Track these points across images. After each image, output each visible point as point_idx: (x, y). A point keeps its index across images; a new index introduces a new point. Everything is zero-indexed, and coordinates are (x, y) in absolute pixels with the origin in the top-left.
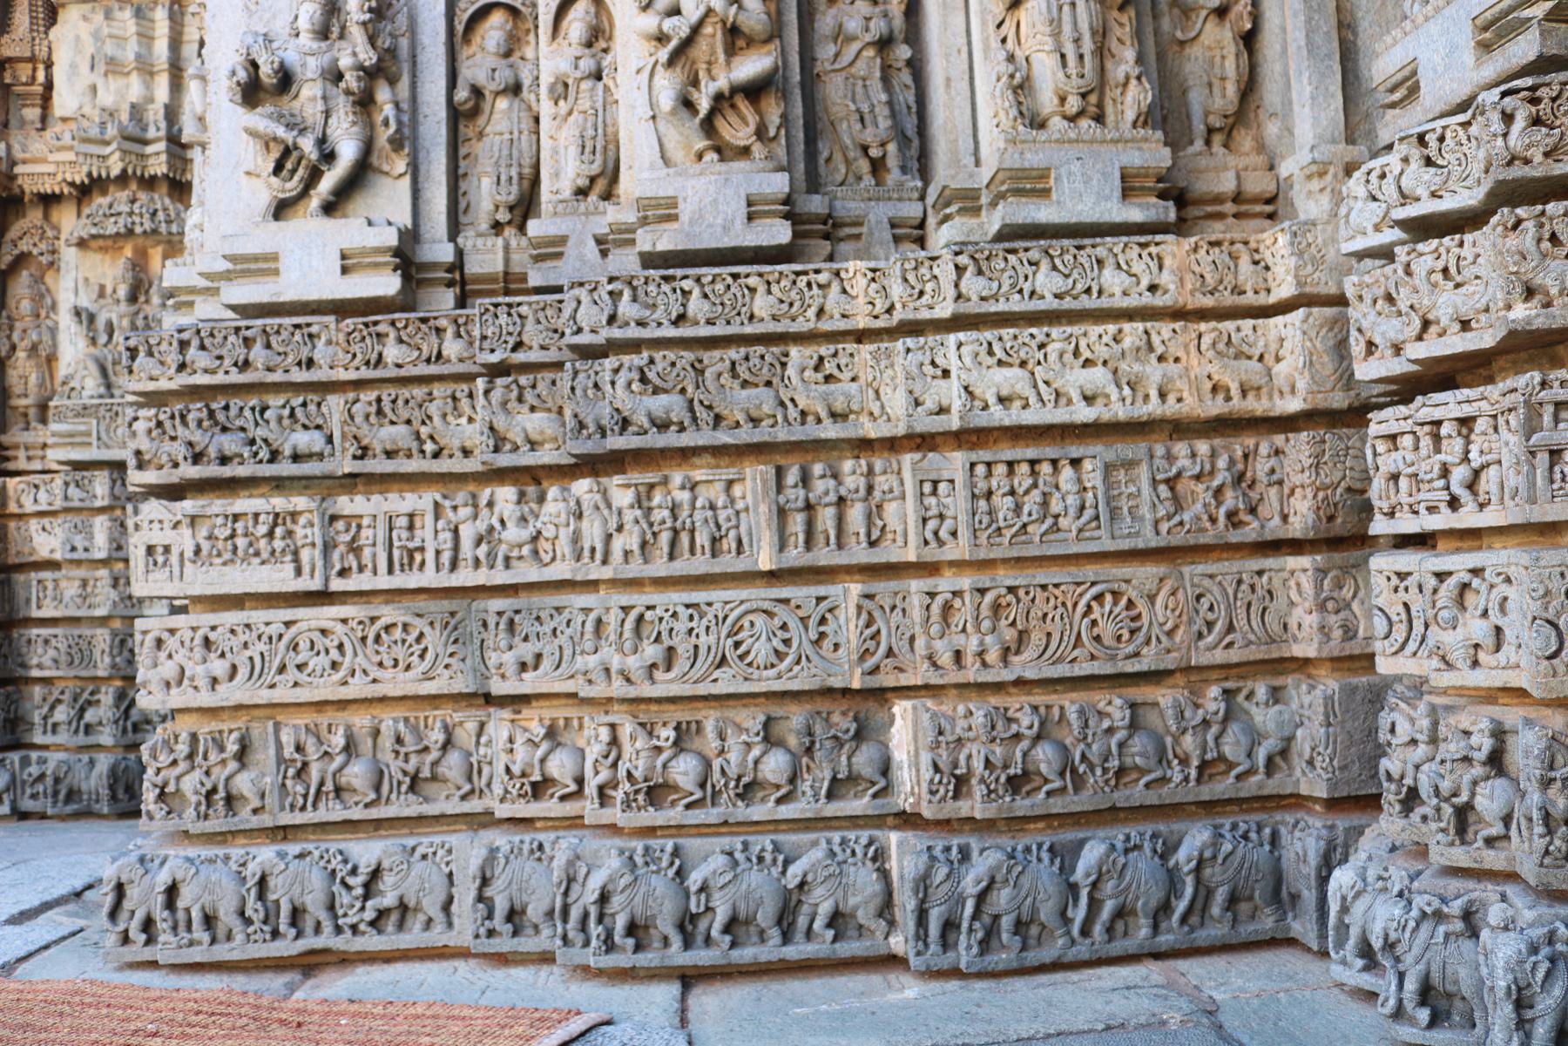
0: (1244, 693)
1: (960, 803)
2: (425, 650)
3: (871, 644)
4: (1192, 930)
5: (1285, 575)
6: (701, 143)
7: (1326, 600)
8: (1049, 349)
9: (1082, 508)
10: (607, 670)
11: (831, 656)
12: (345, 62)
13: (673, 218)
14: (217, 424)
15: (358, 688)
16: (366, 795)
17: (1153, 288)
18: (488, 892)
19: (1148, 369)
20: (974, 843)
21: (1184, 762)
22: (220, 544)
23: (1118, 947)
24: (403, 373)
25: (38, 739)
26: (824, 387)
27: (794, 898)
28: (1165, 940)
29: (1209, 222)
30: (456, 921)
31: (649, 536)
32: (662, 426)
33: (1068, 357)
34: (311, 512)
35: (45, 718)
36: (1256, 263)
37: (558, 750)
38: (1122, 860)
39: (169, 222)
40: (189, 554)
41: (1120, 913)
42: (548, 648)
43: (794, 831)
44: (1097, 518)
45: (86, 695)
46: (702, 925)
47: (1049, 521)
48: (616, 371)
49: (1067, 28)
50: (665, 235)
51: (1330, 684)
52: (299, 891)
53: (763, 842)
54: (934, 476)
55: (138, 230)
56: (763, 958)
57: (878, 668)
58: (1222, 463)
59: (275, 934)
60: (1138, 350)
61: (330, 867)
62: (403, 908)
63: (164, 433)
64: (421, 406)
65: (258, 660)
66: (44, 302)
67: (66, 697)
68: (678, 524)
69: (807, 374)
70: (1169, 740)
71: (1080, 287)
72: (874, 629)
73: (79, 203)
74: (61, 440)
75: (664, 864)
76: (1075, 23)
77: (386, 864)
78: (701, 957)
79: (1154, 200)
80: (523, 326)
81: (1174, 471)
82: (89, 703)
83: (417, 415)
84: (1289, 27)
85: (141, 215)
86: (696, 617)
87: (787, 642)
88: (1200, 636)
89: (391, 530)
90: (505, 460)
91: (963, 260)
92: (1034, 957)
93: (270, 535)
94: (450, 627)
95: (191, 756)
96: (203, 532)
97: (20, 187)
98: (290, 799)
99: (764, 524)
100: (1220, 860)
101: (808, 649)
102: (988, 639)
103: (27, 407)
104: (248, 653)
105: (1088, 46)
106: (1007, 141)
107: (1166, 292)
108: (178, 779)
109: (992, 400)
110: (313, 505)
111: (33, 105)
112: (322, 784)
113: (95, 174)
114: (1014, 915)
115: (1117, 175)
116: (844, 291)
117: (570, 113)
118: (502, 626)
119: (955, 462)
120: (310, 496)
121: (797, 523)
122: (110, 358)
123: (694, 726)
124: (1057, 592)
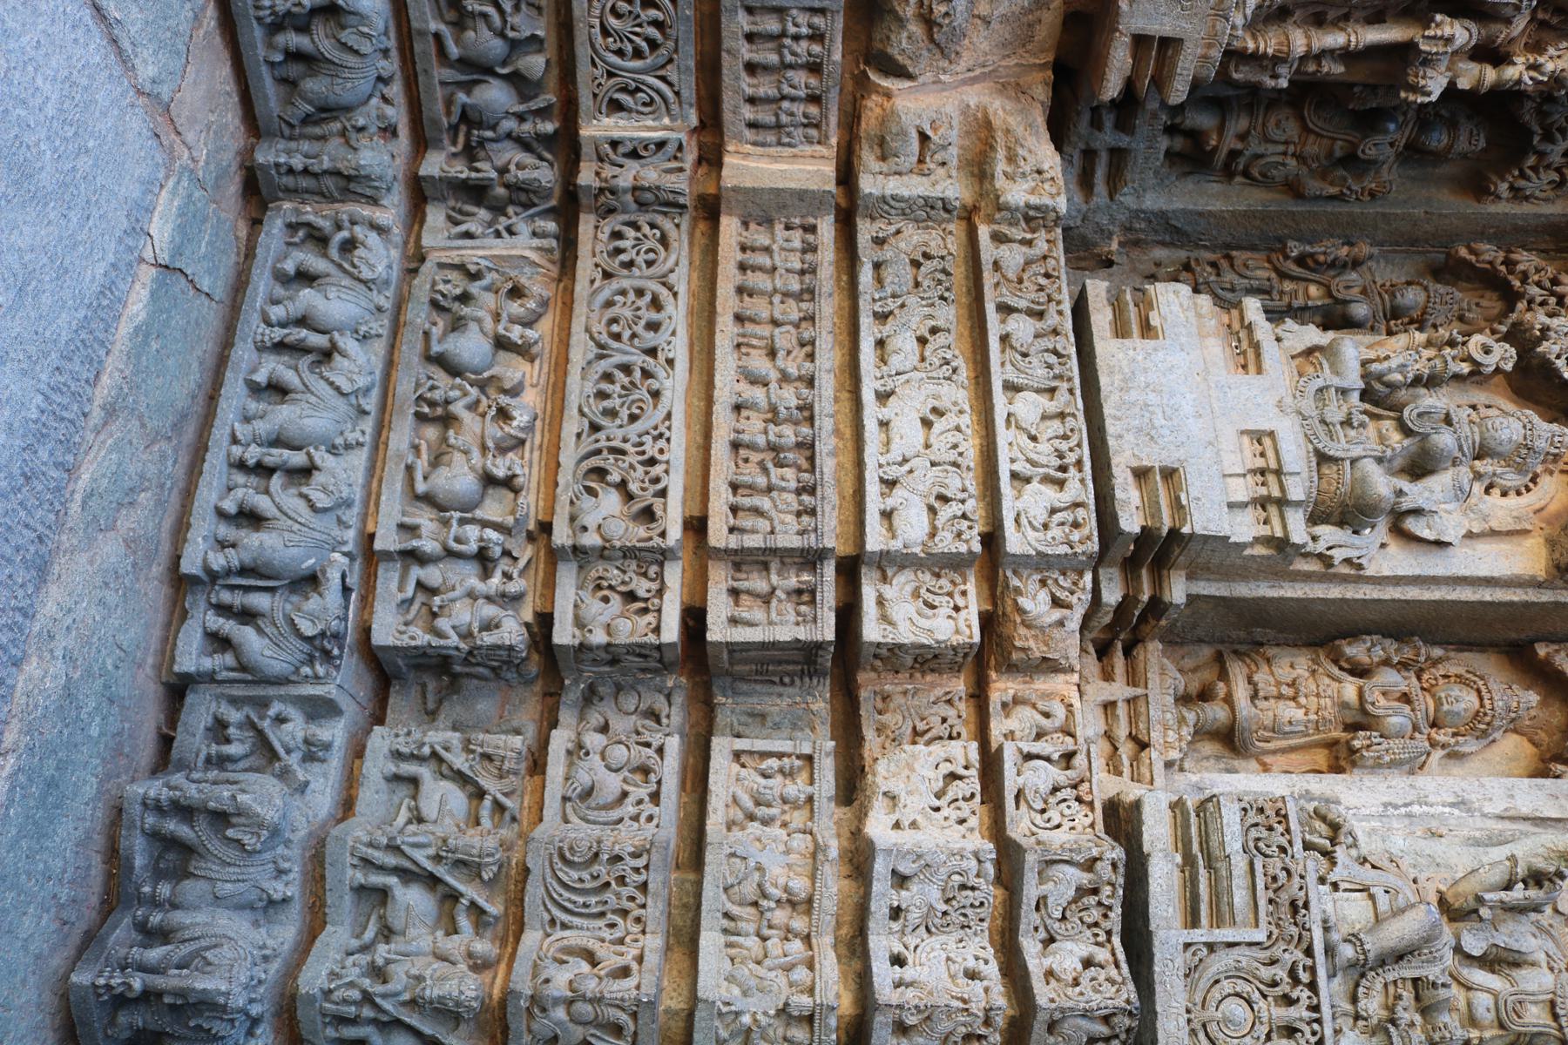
45: (470, 891)
103: (1229, 700)
122: (1433, 972)
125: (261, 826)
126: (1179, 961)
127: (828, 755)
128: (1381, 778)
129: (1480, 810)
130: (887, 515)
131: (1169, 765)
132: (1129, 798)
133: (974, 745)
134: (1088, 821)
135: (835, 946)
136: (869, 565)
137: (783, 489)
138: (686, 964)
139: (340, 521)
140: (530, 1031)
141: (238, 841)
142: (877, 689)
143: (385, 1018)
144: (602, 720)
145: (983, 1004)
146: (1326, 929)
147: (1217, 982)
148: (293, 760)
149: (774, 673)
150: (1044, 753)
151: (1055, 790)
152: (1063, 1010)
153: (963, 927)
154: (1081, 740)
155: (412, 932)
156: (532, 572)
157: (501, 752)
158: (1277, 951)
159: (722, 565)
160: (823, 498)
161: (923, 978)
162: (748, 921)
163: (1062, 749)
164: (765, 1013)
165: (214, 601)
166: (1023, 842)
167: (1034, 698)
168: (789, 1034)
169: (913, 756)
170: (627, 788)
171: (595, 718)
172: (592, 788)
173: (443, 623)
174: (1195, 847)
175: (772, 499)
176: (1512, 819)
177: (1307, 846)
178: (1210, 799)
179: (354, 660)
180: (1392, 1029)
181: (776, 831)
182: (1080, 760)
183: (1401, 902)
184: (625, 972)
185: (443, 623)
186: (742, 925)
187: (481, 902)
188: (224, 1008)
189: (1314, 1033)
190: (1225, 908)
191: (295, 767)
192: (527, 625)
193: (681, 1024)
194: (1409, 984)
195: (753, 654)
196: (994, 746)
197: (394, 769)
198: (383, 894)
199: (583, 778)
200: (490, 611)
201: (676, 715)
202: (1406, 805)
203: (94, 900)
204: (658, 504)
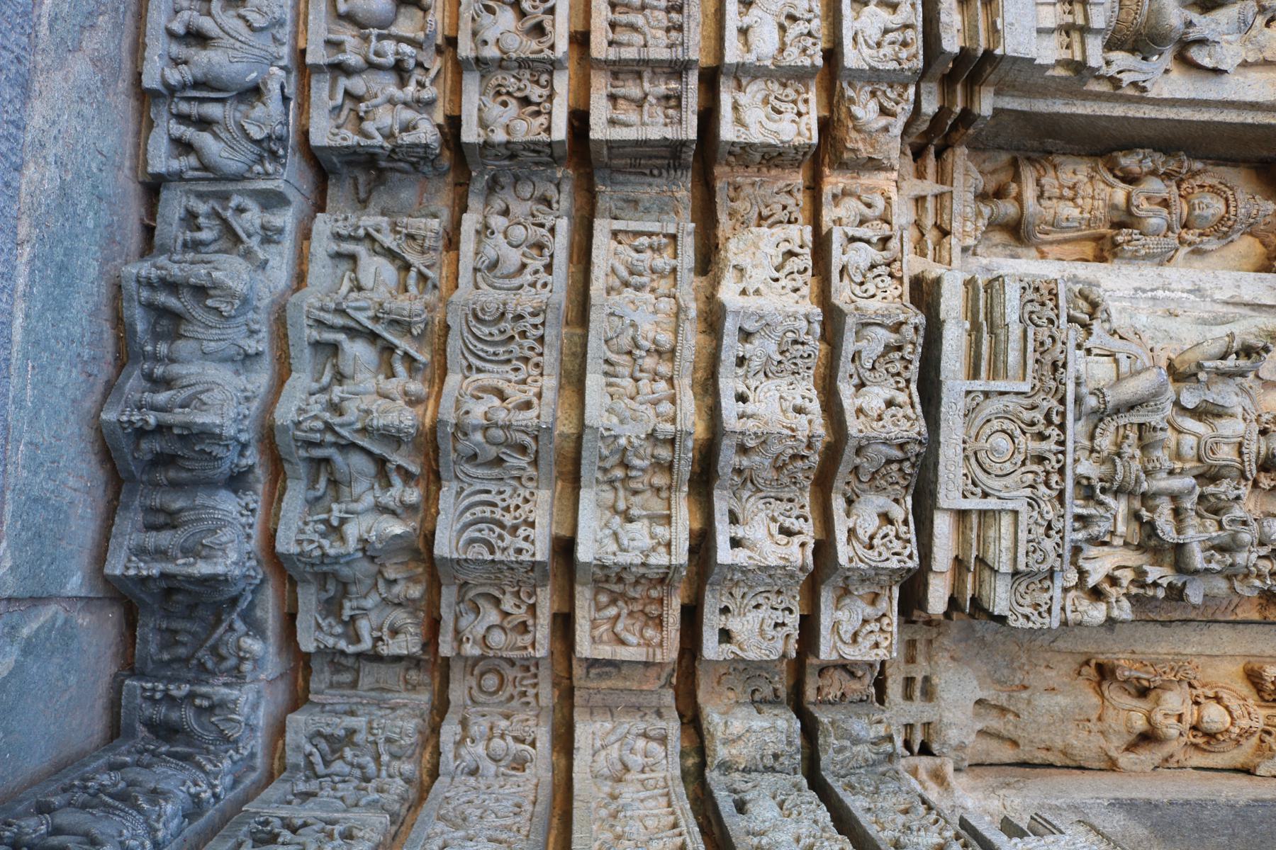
45: (403, 344)
103: (1019, 199)
122: (1155, 420)
125: (233, 296)
126: (961, 404)
127: (689, 234)
128: (1136, 267)
129: (1211, 296)
130: (744, 32)
131: (965, 250)
132: (932, 275)
133: (809, 229)
134: (897, 293)
135: (692, 387)
136: (727, 75)
137: (655, 8)
138: (575, 399)
139: (275, 39)
140: (455, 450)
141: (217, 309)
142: (730, 180)
143: (343, 442)
144: (503, 205)
145: (807, 432)
146: (1078, 384)
147: (989, 421)
148: (254, 243)
149: (645, 166)
150: (865, 237)
151: (873, 267)
152: (868, 439)
153: (794, 373)
154: (896, 227)
155: (359, 377)
156: (441, 81)
157: (423, 233)
158: (1037, 400)
159: (602, 74)
160: (689, 16)
161: (760, 412)
162: (623, 366)
163: (880, 234)
164: (637, 437)
165: (174, 111)
166: (845, 308)
167: (859, 191)
168: (656, 453)
169: (759, 236)
170: (525, 260)
171: (498, 204)
172: (497, 261)
173: (369, 126)
174: (982, 317)
175: (645, 16)
176: (1235, 304)
177: (1071, 319)
178: (997, 279)
179: (297, 158)
180: (1118, 460)
181: (646, 295)
182: (894, 244)
183: (1139, 365)
184: (527, 405)
185: (369, 126)
186: (619, 369)
187: (412, 352)
188: (220, 436)
189: (1058, 461)
190: (1001, 365)
191: (256, 248)
192: (439, 126)
193: (572, 445)
194: (1135, 428)
195: (628, 150)
196: (825, 230)
197: (336, 248)
198: (335, 348)
199: (490, 253)
200: (407, 115)
201: (564, 201)
202: (1152, 290)
203: (109, 357)
204: (547, 20)
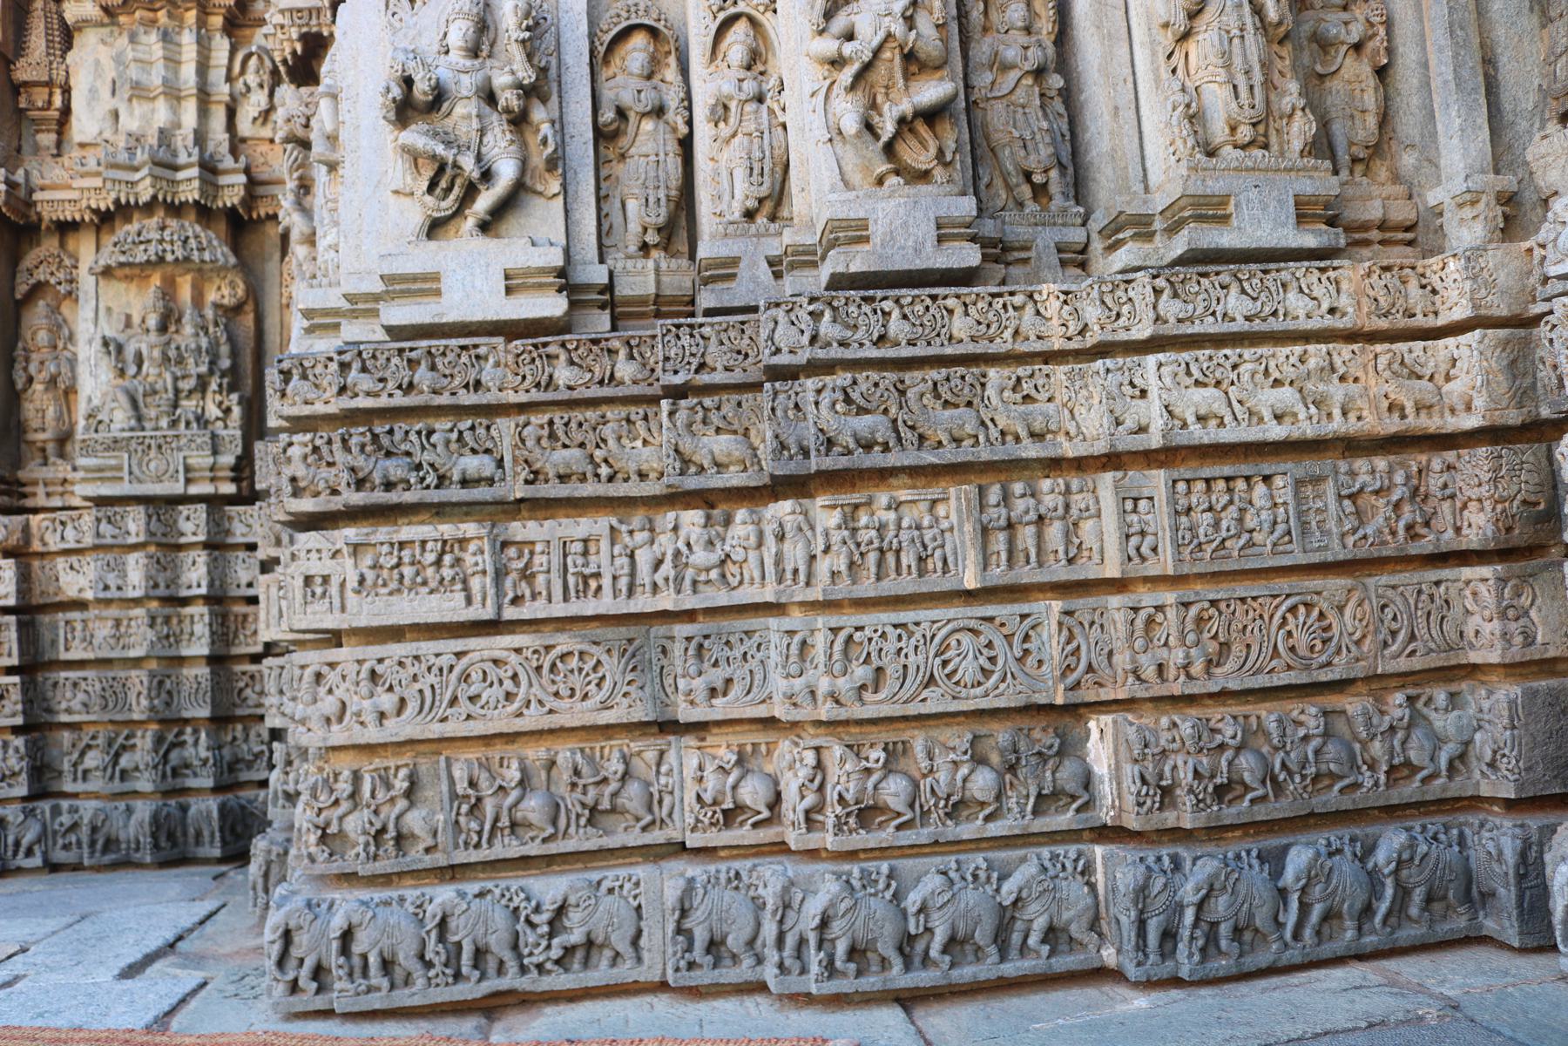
0: (1423, 699)
1: (1166, 814)
2: (603, 678)
3: (1072, 660)
4: (1392, 933)
5: (1460, 585)
6: (884, 167)
7: (1507, 608)
8: (1242, 369)
9: (1275, 523)
10: (813, 693)
11: (1034, 672)
12: (501, 80)
13: (866, 240)
14: (380, 448)
15: (534, 719)
16: (543, 830)
17: (1332, 311)
18: (687, 924)
19: (1331, 389)
20: (1185, 853)
21: (1371, 768)
22: (385, 573)
23: (1327, 950)
24: (575, 395)
25: (68, 787)
26: (1023, 408)
27: (1008, 915)
28: (1370, 941)
29: (1356, 249)
30: (646, 955)
31: (856, 557)
32: (868, 446)
33: (1259, 377)
34: (480, 538)
35: (75, 765)
36: (1423, 287)
37: (749, 777)
38: (1329, 863)
39: (201, 250)
40: (352, 582)
41: (1328, 916)
42: (739, 672)
43: (999, 848)
44: (1289, 533)
45: (120, 740)
46: (920, 947)
47: (1245, 536)
48: (819, 392)
49: (1238, 61)
50: (858, 257)
51: (1508, 691)
52: (482, 931)
53: (978, 860)
54: (1135, 494)
55: (169, 257)
56: (982, 977)
57: (1079, 683)
58: (1399, 478)
59: (458, 976)
60: (1322, 369)
61: (512, 905)
62: (589, 944)
63: (321, 459)
64: (594, 429)
65: (428, 693)
66: (61, 334)
67: (100, 741)
68: (885, 545)
69: (1006, 394)
70: (1357, 746)
71: (1267, 310)
72: (1074, 644)
73: (98, 230)
74: (90, 475)
75: (881, 886)
76: (1245, 56)
77: (572, 900)
78: (923, 978)
79: (1324, 227)
80: (706, 348)
81: (1357, 486)
82: (124, 748)
83: (591, 438)
84: (1433, 63)
85: (172, 242)
86: (905, 638)
87: (992, 660)
88: (1386, 645)
89: (565, 556)
90: (692, 483)
91: (1161, 282)
92: (1250, 963)
93: (438, 563)
94: (628, 655)
95: (354, 795)
96: (367, 560)
97: (39, 214)
98: (463, 836)
99: (968, 543)
100: (1417, 862)
101: (1014, 666)
102: (1193, 651)
103: (44, 442)
104: (417, 686)
105: (1258, 77)
106: (1189, 168)
107: (1344, 315)
108: (341, 819)
109: (1191, 419)
110: (484, 532)
111: (48, 131)
112: (496, 819)
113: (123, 201)
114: (1232, 922)
115: (1292, 202)
116: (1038, 313)
117: (734, 135)
118: (691, 652)
119: (1157, 480)
120: (479, 521)
121: (999, 542)
122: (141, 390)
123: (900, 746)
124: (1255, 605)
185: (17, 769)
199: (78, 707)
200: (11, 751)
